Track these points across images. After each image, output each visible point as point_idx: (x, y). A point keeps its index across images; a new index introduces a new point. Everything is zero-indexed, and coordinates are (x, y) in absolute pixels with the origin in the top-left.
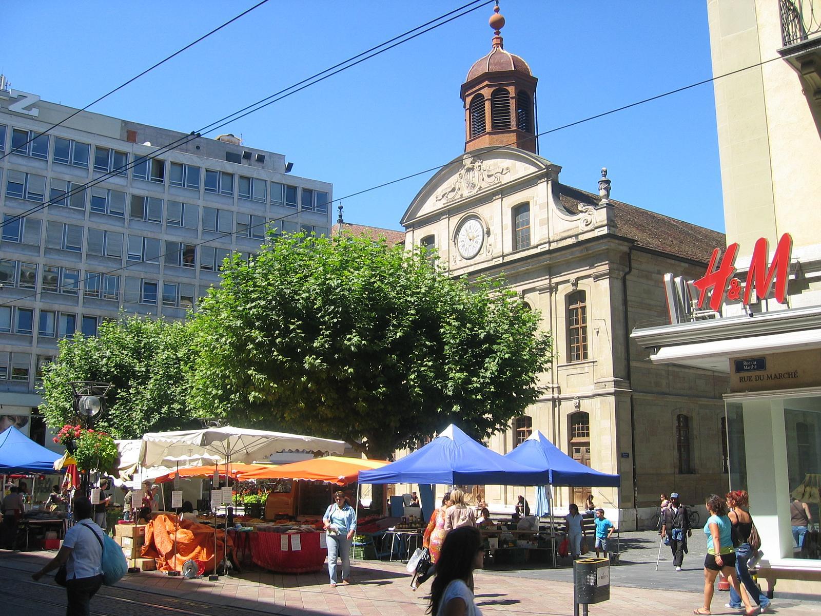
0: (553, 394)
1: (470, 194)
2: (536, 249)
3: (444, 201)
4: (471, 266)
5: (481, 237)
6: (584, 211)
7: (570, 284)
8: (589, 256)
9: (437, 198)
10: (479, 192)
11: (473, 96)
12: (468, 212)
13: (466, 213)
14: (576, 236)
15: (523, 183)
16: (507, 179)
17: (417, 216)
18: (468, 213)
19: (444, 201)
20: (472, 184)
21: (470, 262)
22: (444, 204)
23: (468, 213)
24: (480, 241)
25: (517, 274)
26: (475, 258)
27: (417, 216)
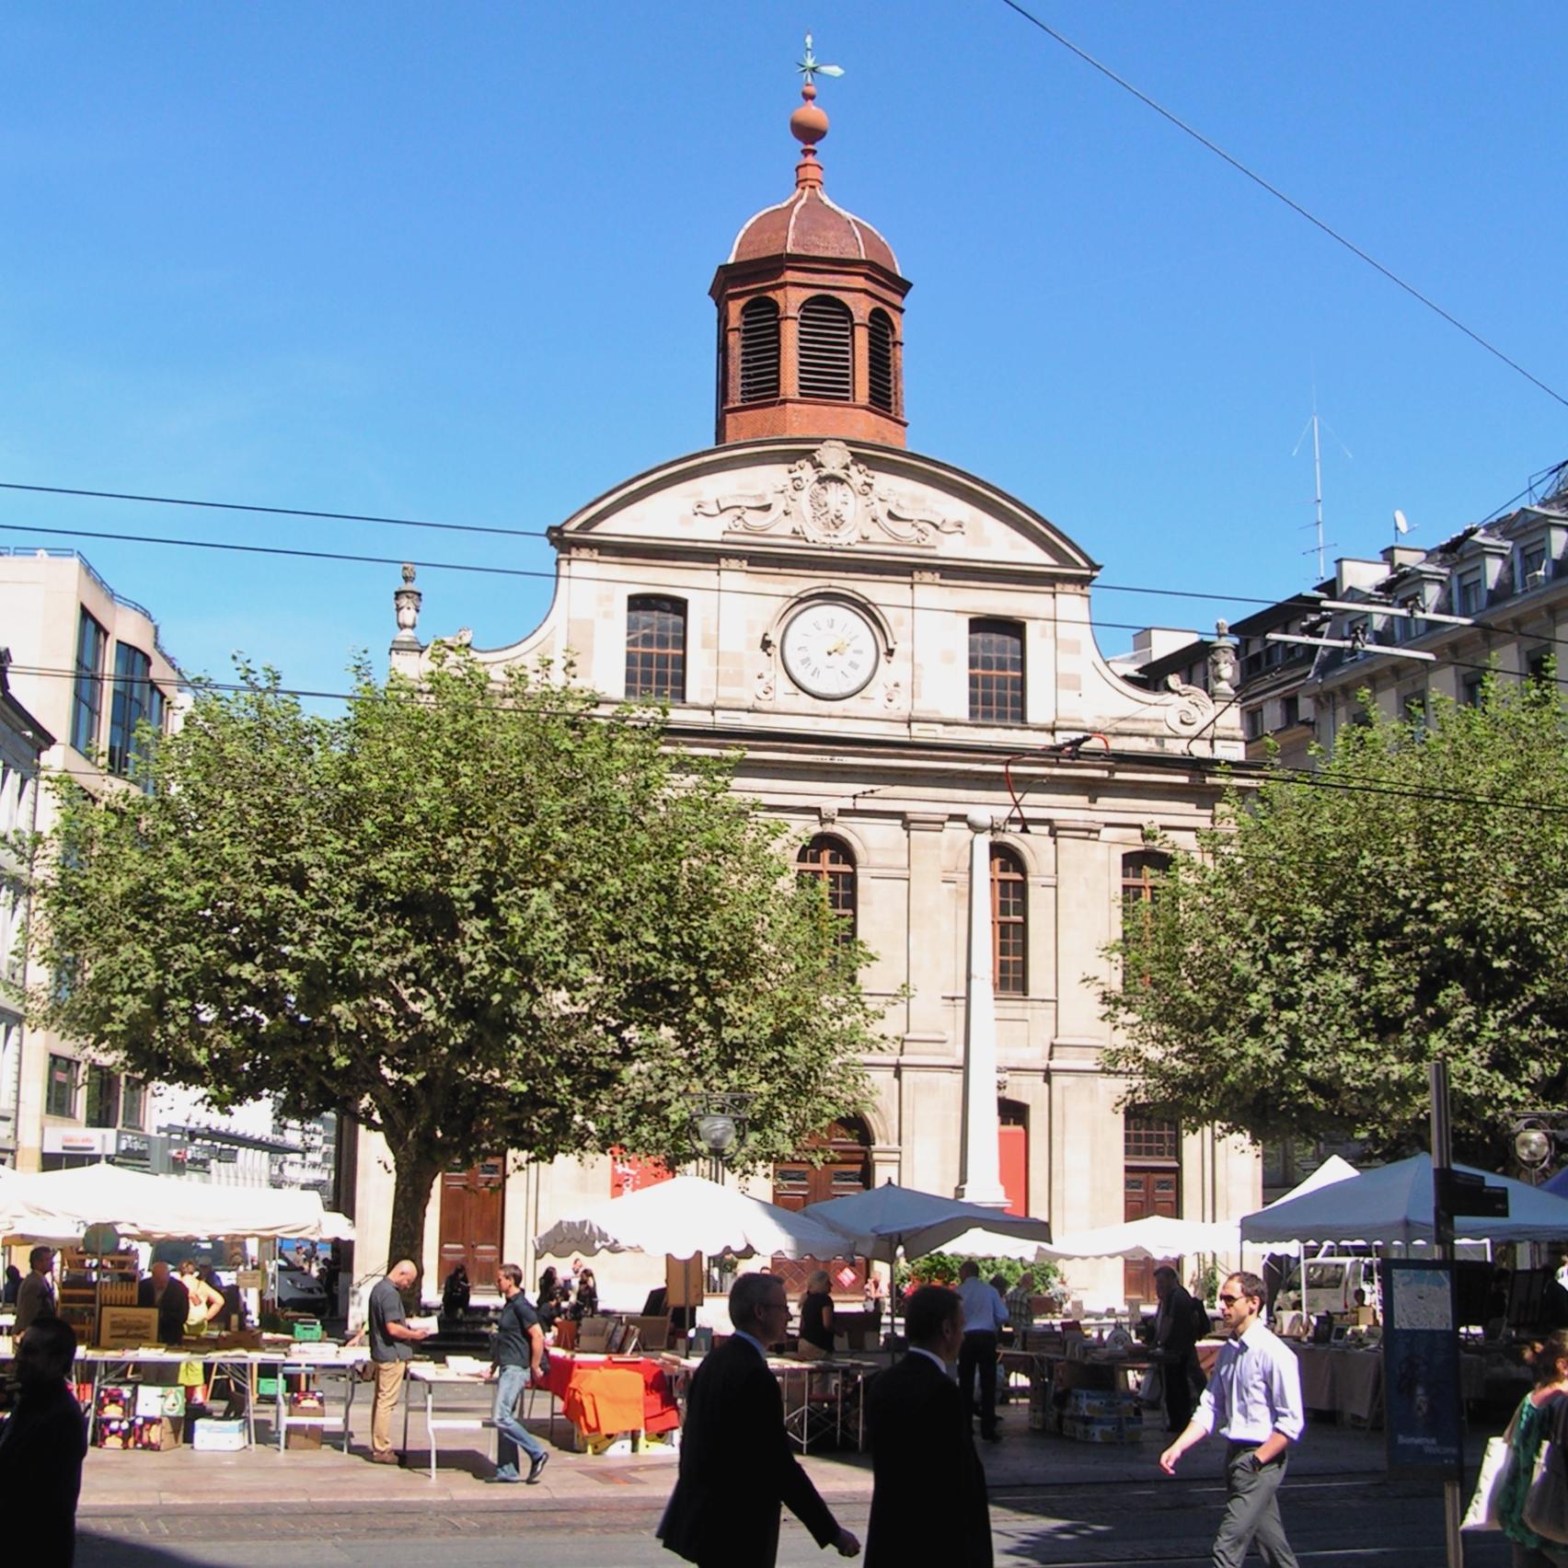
1: (828, 540)
3: (725, 521)
11: (748, 298)
12: (834, 583)
14: (1160, 739)
16: (951, 548)
19: (725, 521)
20: (837, 517)
21: (806, 703)
22: (724, 533)
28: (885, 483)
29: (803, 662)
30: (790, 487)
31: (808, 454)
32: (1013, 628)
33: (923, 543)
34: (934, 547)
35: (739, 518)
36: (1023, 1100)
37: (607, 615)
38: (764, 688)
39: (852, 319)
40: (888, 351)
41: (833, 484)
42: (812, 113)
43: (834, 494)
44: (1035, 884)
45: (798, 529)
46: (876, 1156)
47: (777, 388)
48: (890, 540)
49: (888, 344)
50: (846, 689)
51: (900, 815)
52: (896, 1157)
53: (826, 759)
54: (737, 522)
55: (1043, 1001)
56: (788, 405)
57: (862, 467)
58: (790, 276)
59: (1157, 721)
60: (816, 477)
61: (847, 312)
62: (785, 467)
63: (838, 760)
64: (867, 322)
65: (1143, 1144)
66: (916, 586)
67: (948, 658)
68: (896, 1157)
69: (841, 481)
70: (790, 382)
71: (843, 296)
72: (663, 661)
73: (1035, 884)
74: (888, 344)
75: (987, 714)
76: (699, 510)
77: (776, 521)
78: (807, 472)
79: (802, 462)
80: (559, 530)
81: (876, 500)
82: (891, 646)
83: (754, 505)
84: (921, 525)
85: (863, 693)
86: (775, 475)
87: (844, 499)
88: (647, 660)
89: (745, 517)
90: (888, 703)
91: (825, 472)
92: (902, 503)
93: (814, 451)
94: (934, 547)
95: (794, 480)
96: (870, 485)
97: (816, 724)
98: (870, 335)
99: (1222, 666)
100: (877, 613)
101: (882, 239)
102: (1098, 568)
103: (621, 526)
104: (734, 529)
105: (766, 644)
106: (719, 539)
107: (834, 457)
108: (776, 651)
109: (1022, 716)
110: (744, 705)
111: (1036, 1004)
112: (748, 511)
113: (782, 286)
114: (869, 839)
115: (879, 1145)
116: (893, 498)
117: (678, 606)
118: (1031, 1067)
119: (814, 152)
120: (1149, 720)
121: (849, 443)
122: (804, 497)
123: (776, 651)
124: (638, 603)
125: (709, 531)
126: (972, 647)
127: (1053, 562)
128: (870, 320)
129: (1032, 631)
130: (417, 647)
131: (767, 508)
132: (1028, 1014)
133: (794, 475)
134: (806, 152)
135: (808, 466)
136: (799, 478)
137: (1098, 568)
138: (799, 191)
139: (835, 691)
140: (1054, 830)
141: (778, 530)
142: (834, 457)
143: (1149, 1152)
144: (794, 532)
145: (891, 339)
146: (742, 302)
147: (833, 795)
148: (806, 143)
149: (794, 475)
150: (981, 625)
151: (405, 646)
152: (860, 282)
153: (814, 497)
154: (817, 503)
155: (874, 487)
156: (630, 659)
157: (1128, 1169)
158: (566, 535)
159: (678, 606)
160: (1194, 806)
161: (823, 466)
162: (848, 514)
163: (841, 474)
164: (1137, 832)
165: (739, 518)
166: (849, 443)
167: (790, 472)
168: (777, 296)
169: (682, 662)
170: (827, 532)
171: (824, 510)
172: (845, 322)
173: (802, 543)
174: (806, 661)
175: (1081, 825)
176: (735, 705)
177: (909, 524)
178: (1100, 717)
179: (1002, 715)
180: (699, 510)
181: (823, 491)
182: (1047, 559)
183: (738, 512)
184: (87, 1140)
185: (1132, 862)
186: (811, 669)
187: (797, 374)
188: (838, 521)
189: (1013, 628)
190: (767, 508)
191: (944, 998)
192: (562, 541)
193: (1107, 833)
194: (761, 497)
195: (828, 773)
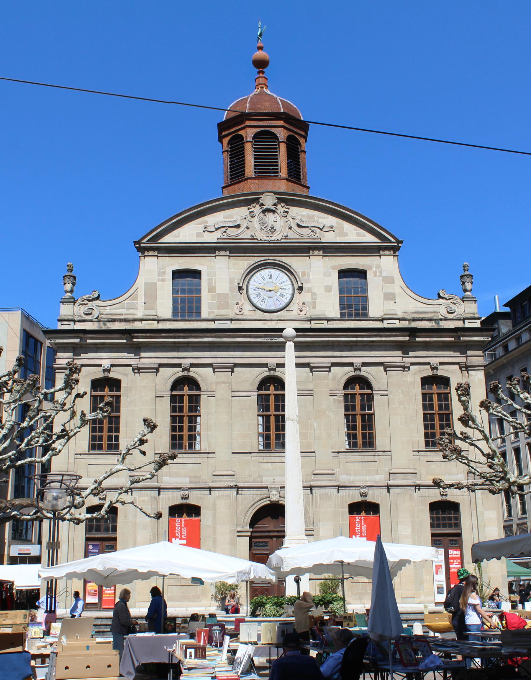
0: (468, 479)
1: (267, 239)
2: (213, 322)
3: (218, 234)
4: (271, 320)
5: (290, 292)
6: (448, 298)
7: (101, 369)
8: (223, 344)
9: (205, 228)
10: (283, 241)
12: (272, 258)
13: (267, 258)
14: (437, 321)
15: (336, 249)
16: (328, 238)
17: (159, 242)
18: (269, 260)
19: (218, 234)
20: (272, 228)
21: (259, 315)
22: (218, 239)
23: (269, 260)
24: (289, 297)
25: (281, 344)
26: (279, 313)
27: (159, 242)
28: (294, 211)
29: (257, 296)
30: (249, 217)
31: (256, 200)
32: (361, 274)
33: (314, 237)
34: (320, 239)
35: (225, 232)
36: (376, 501)
37: (163, 280)
38: (239, 309)
39: (278, 140)
40: (299, 155)
41: (270, 214)
42: (260, 54)
43: (270, 217)
44: (377, 394)
45: (254, 235)
47: (244, 174)
48: (298, 237)
49: (299, 152)
50: (279, 307)
53: (269, 340)
54: (224, 234)
55: (384, 452)
56: (249, 181)
57: (283, 204)
58: (248, 123)
59: (434, 312)
60: (261, 210)
61: (275, 136)
62: (246, 208)
63: (274, 340)
64: (285, 140)
65: (441, 522)
67: (328, 289)
69: (274, 212)
70: (250, 169)
71: (274, 130)
72: (191, 300)
73: (377, 394)
74: (299, 152)
75: (350, 315)
76: (206, 230)
77: (242, 233)
78: (257, 209)
79: (254, 205)
80: (139, 242)
81: (290, 219)
82: (300, 285)
83: (231, 225)
84: (313, 229)
85: (287, 308)
86: (243, 211)
87: (275, 219)
88: (183, 300)
89: (227, 231)
90: (299, 312)
91: (264, 207)
92: (303, 219)
93: (259, 198)
94: (320, 239)
95: (250, 212)
96: (287, 212)
97: (265, 324)
98: (287, 147)
99: (466, 284)
100: (292, 271)
101: (295, 106)
102: (402, 242)
103: (170, 239)
104: (223, 237)
105: (240, 288)
106: (216, 241)
107: (269, 200)
108: (244, 292)
109: (366, 314)
110: (229, 317)
112: (229, 229)
113: (243, 128)
116: (299, 217)
117: (196, 274)
118: (379, 485)
119: (263, 72)
120: (431, 312)
121: (275, 193)
122: (255, 220)
123: (244, 292)
124: (177, 274)
125: (212, 238)
126: (339, 285)
127: (380, 241)
128: (287, 141)
129: (369, 275)
130: (73, 300)
131: (238, 226)
132: (377, 459)
133: (250, 210)
134: (259, 73)
135: (258, 206)
136: (252, 212)
137: (402, 242)
138: (256, 90)
139: (273, 308)
140: (386, 368)
142: (269, 200)
143: (444, 526)
144: (252, 236)
145: (300, 150)
146: (228, 139)
148: (259, 69)
149: (250, 210)
150: (343, 273)
151: (67, 300)
152: (281, 123)
153: (260, 220)
154: (262, 223)
155: (290, 213)
156: (174, 300)
157: (433, 535)
158: (142, 245)
159: (196, 274)
160: (459, 353)
161: (264, 205)
162: (277, 226)
163: (273, 208)
164: (429, 367)
165: (225, 232)
166: (275, 193)
167: (249, 209)
168: (241, 133)
169: (199, 299)
170: (267, 235)
171: (266, 225)
172: (275, 142)
173: (256, 241)
174: (258, 295)
175: (398, 364)
176: (225, 317)
177: (308, 229)
178: (406, 312)
179: (357, 315)
180: (206, 230)
181: (265, 217)
182: (376, 240)
183: (224, 229)
184: (28, 550)
185: (426, 381)
187: (253, 167)
188: (273, 230)
189: (361, 274)
190: (238, 226)
191: (332, 452)
192: (142, 250)
195: (271, 347)
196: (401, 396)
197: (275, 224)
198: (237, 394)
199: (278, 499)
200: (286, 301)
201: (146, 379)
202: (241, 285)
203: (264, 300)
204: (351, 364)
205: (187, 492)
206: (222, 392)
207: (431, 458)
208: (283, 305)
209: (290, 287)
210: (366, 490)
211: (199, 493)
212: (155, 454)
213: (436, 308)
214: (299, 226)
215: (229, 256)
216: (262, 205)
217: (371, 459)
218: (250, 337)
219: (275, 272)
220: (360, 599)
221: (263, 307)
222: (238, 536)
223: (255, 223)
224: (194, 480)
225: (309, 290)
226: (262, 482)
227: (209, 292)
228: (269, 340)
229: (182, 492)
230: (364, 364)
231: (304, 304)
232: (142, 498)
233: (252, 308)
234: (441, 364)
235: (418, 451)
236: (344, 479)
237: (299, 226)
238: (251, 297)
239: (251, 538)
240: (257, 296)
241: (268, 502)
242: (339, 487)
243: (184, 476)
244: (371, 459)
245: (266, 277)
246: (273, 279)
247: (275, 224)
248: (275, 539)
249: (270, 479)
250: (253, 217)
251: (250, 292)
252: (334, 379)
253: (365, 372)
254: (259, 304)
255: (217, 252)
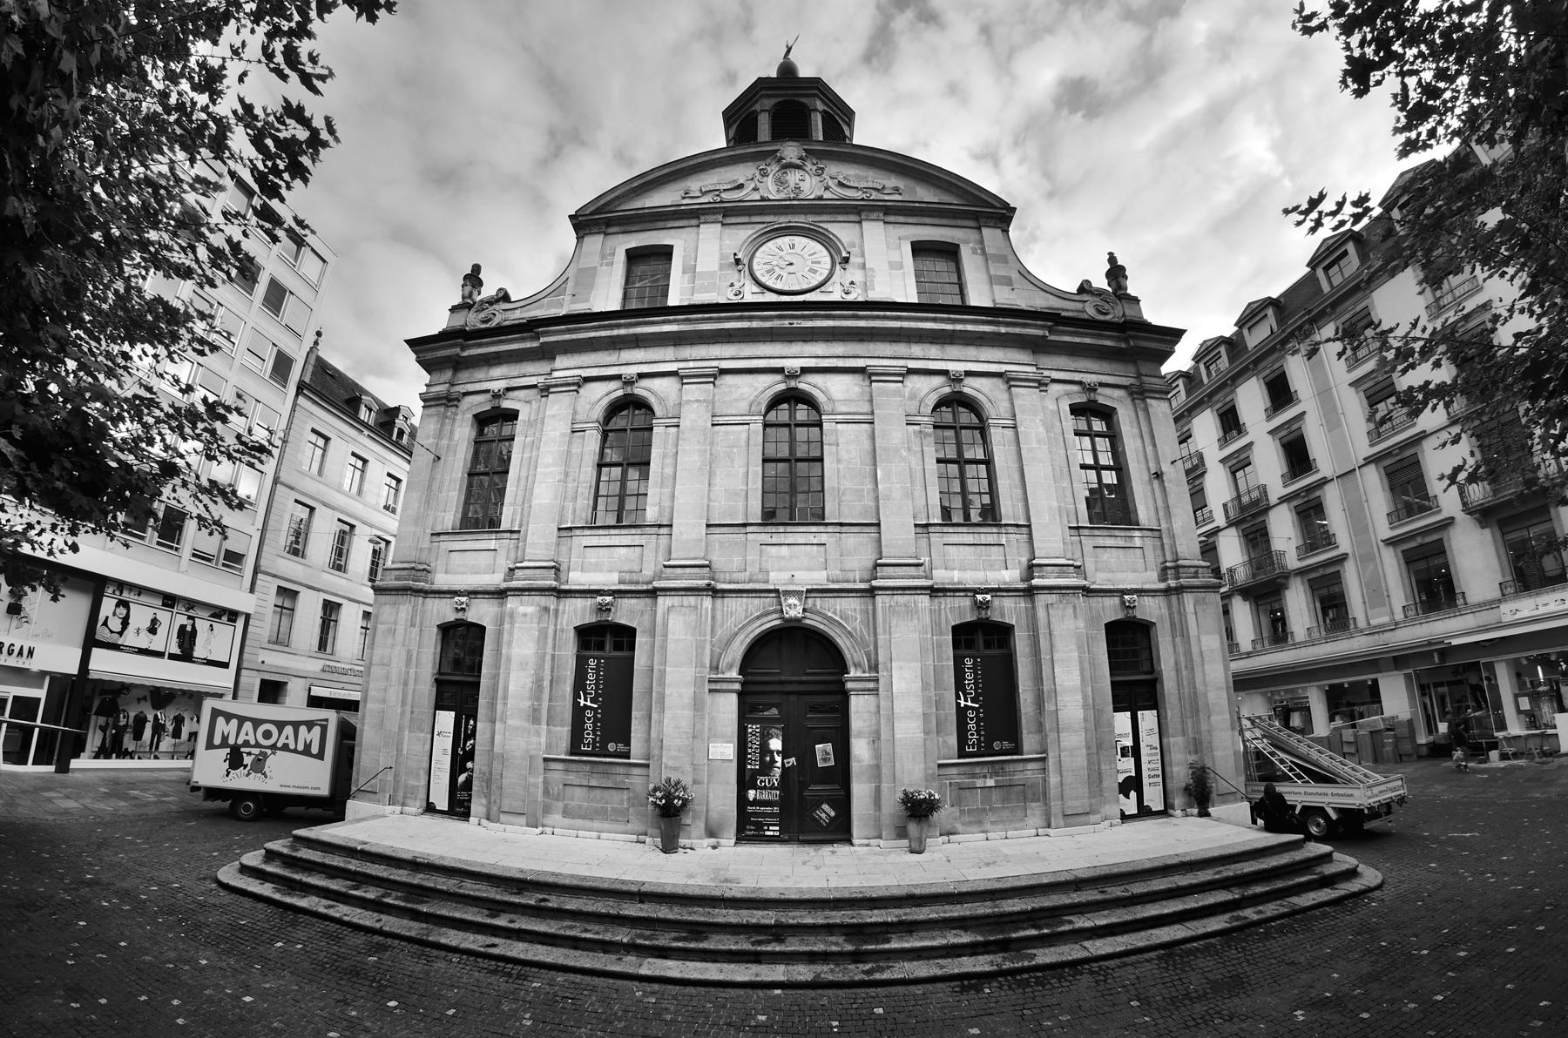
24: (826, 273)
29: (768, 272)
30: (758, 177)
43: (793, 177)
46: (849, 685)
50: (805, 287)
51: (860, 371)
52: (871, 685)
53: (786, 323)
66: (864, 223)
68: (871, 685)
78: (773, 169)
82: (844, 254)
85: (823, 289)
105: (738, 262)
111: (1011, 529)
114: (836, 391)
115: (853, 673)
122: (770, 181)
131: (741, 186)
141: (748, 195)
147: (795, 356)
154: (781, 183)
163: (799, 162)
186: (775, 275)
189: (950, 252)
190: (741, 186)
193: (1055, 388)
194: (734, 181)
196: (1041, 430)
197: (801, 184)
198: (721, 420)
199: (800, 615)
200: (820, 278)
201: (558, 408)
202: (739, 256)
203: (780, 277)
204: (945, 373)
205: (609, 599)
206: (694, 417)
207: (1101, 541)
208: (814, 283)
209: (828, 259)
210: (988, 597)
211: (633, 601)
212: (559, 529)
213: (1079, 306)
214: (841, 184)
215: (723, 225)
216: (782, 158)
217: (991, 539)
218: (750, 318)
219: (800, 241)
220: (980, 822)
221: (779, 286)
222: (711, 691)
223: (769, 183)
224: (627, 577)
225: (863, 266)
226: (767, 582)
227: (684, 272)
228: (786, 323)
229: (599, 599)
230: (969, 374)
231: (852, 283)
232: (522, 609)
233: (756, 289)
234: (1102, 385)
235: (1078, 528)
236: (941, 577)
237: (841, 184)
238: (758, 274)
239: (740, 694)
240: (768, 272)
241: (778, 622)
242: (934, 592)
243: (610, 571)
244: (991, 539)
245: (786, 248)
246: (798, 249)
247: (801, 184)
248: (793, 698)
249: (786, 576)
250: (765, 175)
251: (755, 267)
252: (913, 396)
253: (971, 387)
254: (770, 283)
255: (702, 218)
